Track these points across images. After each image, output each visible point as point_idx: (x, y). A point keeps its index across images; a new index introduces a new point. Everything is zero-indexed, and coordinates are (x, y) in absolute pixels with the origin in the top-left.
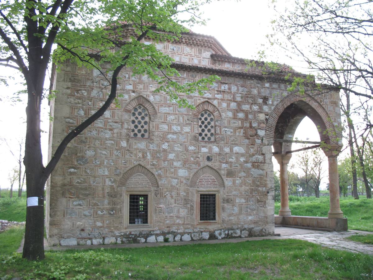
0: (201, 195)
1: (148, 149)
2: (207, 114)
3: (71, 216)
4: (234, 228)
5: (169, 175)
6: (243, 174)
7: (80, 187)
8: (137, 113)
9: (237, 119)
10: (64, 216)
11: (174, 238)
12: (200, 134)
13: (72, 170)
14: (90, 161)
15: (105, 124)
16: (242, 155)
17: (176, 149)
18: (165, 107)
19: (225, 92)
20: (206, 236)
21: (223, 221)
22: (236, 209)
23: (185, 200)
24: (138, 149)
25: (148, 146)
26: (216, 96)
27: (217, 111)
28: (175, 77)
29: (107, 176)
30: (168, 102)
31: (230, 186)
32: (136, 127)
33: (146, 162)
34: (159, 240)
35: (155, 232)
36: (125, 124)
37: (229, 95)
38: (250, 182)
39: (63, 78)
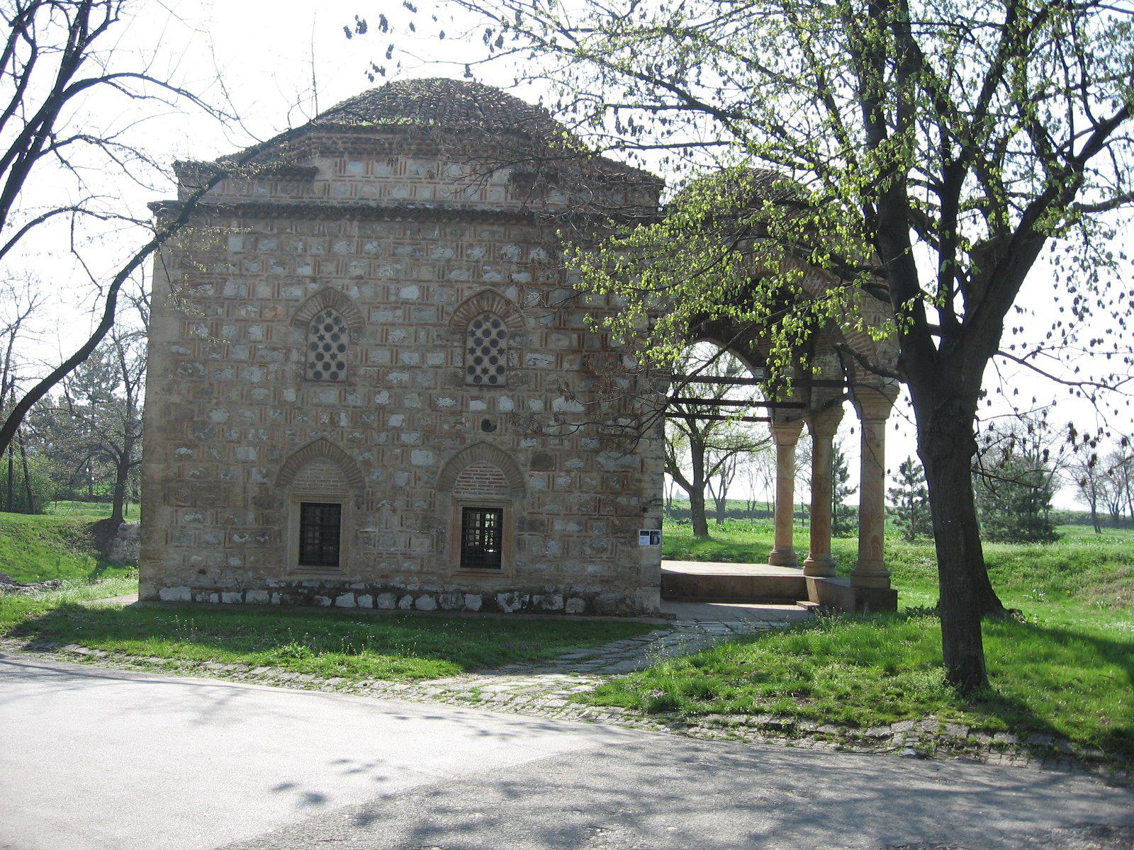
0: (465, 509)
4: (547, 589)
7: (198, 484)
8: (321, 327)
11: (397, 602)
12: (472, 370)
13: (183, 450)
17: (407, 403)
20: (474, 602)
21: (518, 571)
22: (554, 547)
23: (425, 518)
29: (253, 462)
30: (393, 298)
31: (540, 491)
32: (320, 357)
34: (361, 604)
36: (294, 351)
38: (594, 483)
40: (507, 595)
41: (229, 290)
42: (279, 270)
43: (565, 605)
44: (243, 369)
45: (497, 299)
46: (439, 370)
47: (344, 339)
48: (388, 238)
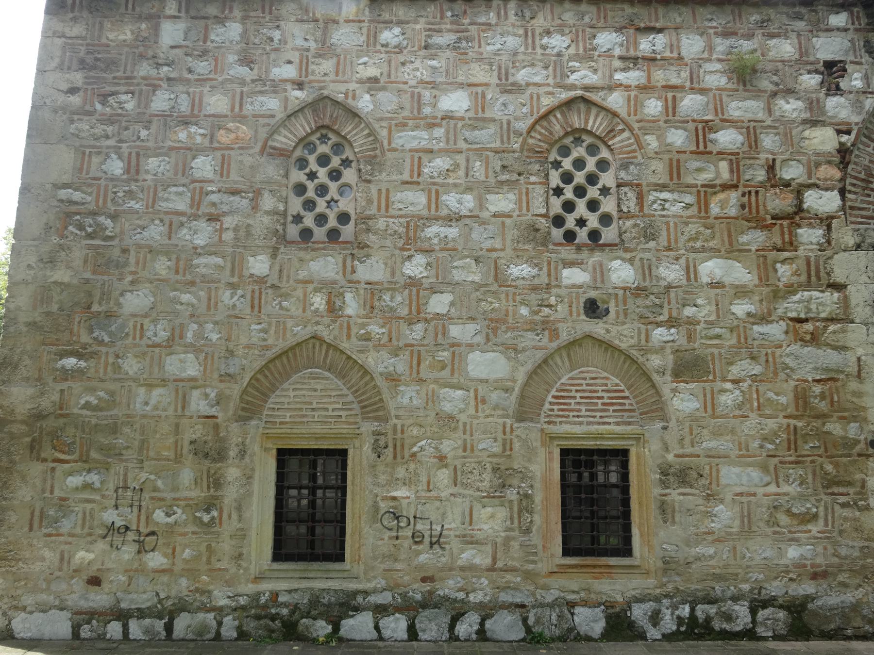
0: (564, 452)
1: (350, 282)
2: (585, 144)
3: (56, 528)
4: (719, 593)
5: (431, 375)
7: (94, 421)
8: (312, 159)
9: (710, 153)
10: (31, 529)
11: (452, 627)
12: (558, 221)
14: (135, 327)
15: (192, 199)
16: (741, 292)
17: (458, 276)
18: (417, 127)
19: (654, 60)
20: (590, 621)
22: (725, 515)
23: (495, 470)
24: (311, 282)
25: (349, 269)
26: (618, 76)
27: (623, 130)
28: (452, 23)
29: (193, 379)
30: (427, 110)
31: (692, 417)
32: (310, 205)
33: (341, 326)
34: (386, 633)
35: (373, 599)
37: (673, 68)
38: (783, 400)
39: (57, 60)
40: (649, 606)
41: (160, 102)
42: (243, 71)
43: (754, 621)
44: (182, 224)
45: (594, 111)
46: (508, 221)
47: (349, 175)
48: (416, 22)
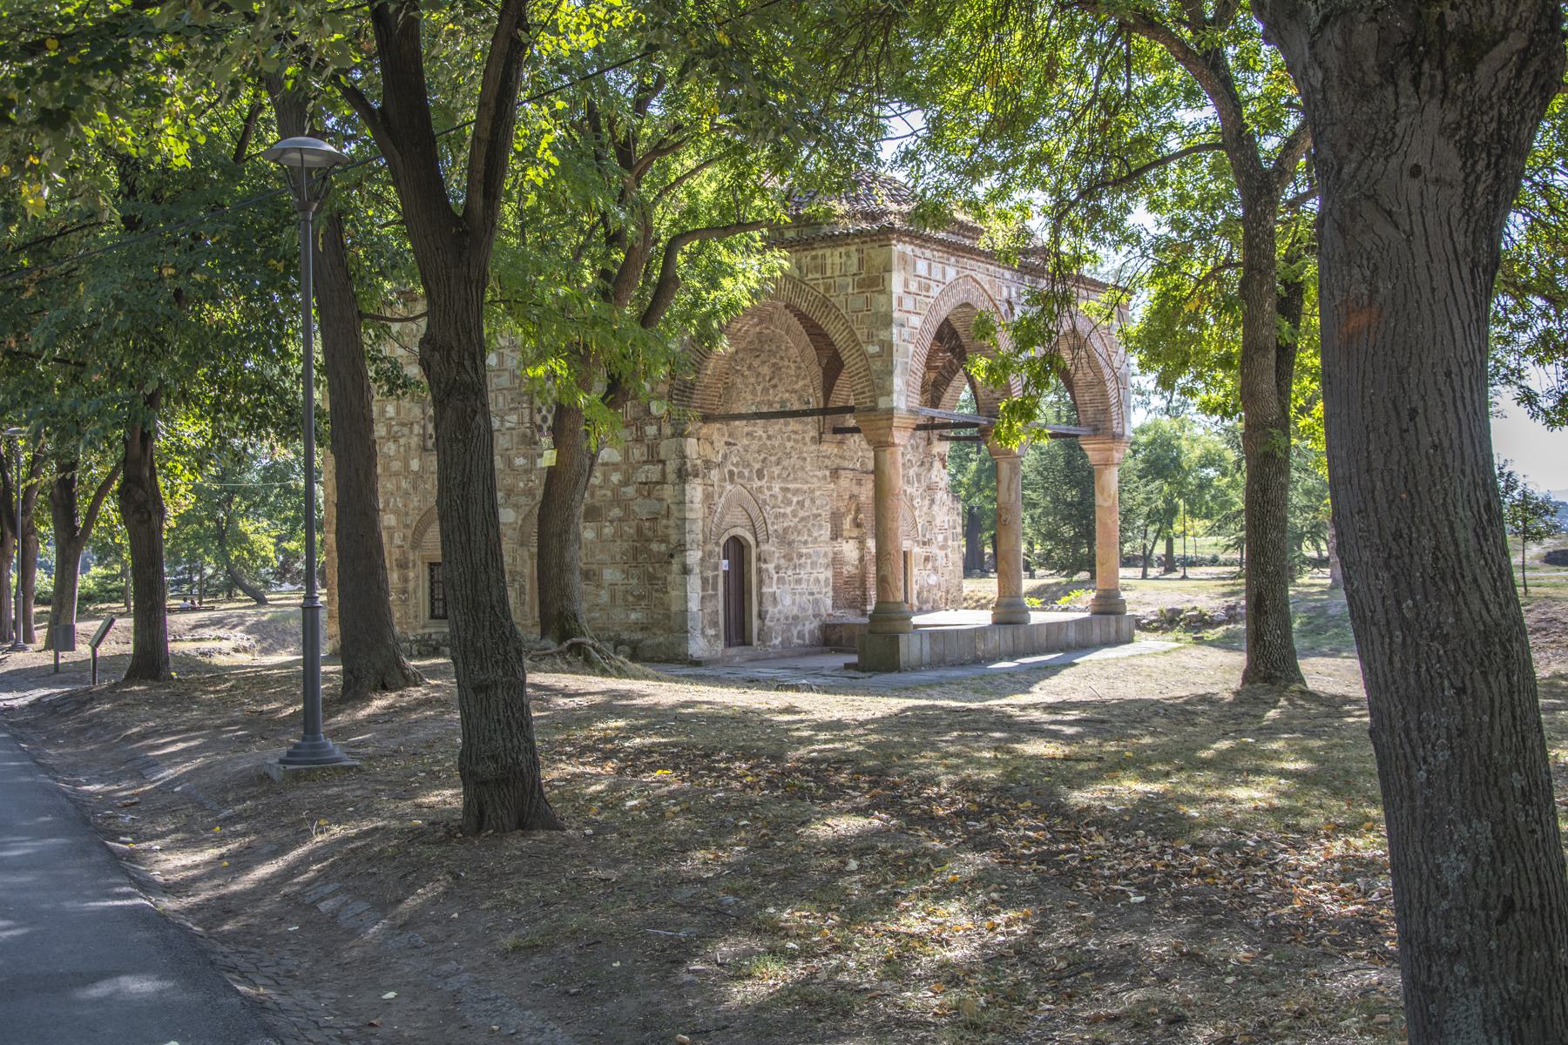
6: (616, 512)
16: (615, 467)
22: (604, 596)
31: (592, 542)
